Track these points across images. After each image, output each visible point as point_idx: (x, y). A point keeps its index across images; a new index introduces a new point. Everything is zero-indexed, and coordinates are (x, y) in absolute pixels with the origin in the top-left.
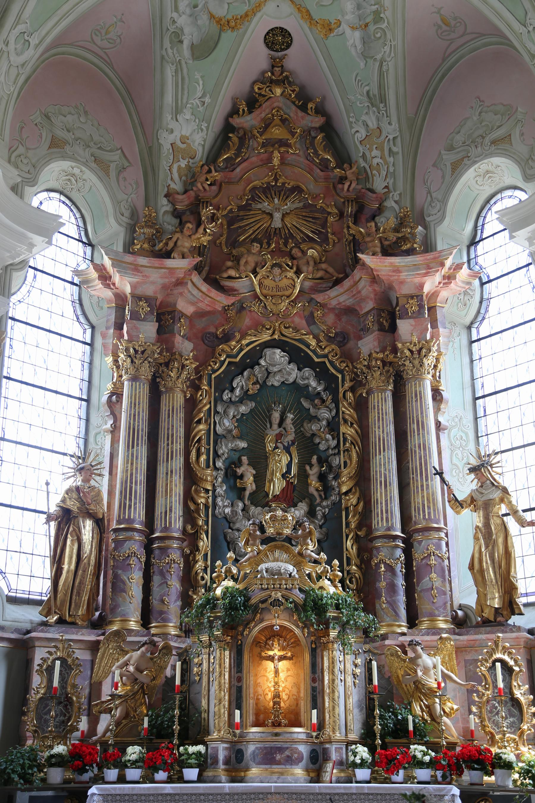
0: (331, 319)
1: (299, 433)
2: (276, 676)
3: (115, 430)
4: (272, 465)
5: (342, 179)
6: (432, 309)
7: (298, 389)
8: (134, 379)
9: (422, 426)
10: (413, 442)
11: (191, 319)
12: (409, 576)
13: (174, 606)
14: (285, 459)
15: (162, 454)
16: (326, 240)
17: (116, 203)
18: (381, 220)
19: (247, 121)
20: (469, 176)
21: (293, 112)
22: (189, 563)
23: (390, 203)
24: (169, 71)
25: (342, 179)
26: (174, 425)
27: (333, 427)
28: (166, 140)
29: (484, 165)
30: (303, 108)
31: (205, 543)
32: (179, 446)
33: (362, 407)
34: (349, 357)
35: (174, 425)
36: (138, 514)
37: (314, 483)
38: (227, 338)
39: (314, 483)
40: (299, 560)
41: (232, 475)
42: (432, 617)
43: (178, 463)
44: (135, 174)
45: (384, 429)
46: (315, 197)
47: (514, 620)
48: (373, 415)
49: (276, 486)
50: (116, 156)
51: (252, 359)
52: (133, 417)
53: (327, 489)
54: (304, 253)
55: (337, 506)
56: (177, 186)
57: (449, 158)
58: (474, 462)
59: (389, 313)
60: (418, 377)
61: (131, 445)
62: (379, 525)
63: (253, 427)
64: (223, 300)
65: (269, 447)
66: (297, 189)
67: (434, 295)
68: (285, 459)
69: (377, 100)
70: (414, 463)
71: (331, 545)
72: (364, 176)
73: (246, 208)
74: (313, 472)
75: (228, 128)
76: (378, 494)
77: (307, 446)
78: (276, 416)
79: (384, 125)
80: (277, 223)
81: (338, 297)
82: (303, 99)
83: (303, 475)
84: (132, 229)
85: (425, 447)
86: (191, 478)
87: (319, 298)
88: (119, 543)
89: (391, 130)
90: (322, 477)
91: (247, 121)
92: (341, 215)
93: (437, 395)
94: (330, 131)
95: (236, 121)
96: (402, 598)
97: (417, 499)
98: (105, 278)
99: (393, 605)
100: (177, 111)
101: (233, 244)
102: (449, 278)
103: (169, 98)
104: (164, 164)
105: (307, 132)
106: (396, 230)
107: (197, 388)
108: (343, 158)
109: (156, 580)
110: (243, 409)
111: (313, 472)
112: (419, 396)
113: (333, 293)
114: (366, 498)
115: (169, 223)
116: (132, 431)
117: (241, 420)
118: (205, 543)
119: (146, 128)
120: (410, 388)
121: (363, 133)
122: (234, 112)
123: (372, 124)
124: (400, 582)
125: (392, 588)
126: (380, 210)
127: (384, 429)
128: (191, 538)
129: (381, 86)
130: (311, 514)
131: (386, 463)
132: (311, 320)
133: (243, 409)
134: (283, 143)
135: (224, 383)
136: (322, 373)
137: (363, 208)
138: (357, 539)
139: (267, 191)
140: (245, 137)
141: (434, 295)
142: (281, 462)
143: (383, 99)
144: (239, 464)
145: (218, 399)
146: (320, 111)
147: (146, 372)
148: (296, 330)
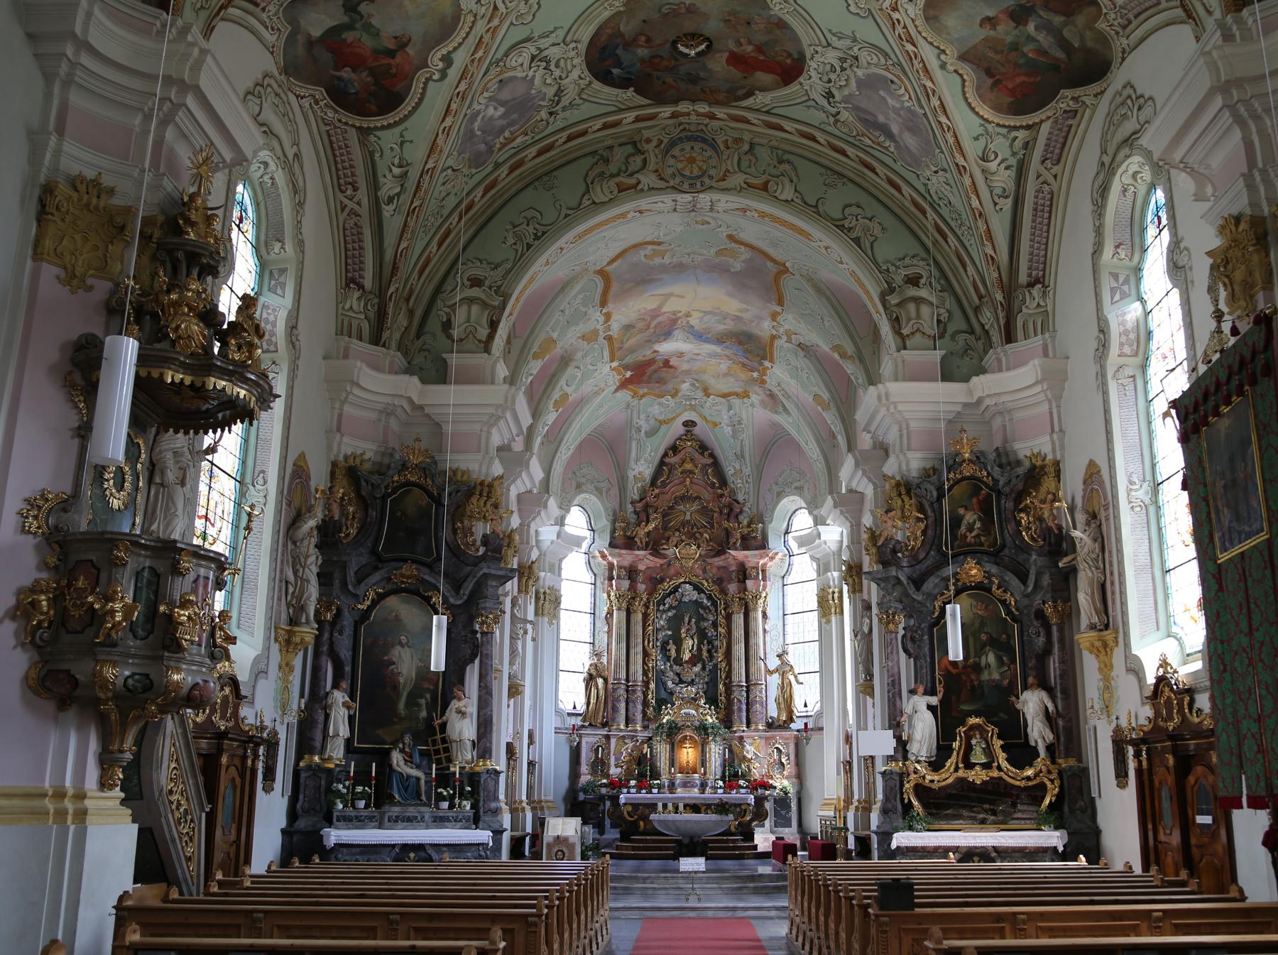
0: (714, 570)
1: (698, 627)
2: (688, 754)
3: (609, 632)
4: (685, 646)
5: (722, 496)
6: (764, 571)
7: (698, 604)
8: (619, 609)
9: (756, 634)
10: (752, 641)
11: (644, 572)
12: (748, 704)
13: (639, 717)
14: (691, 643)
15: (632, 644)
16: (712, 527)
17: (606, 509)
18: (741, 518)
19: (672, 460)
20: (785, 501)
21: (696, 455)
22: (645, 695)
23: (746, 509)
24: (634, 444)
25: (722, 496)
26: (638, 629)
27: (715, 625)
28: (631, 474)
29: (792, 498)
30: (702, 454)
31: (652, 686)
32: (640, 640)
33: (729, 618)
34: (724, 592)
35: (638, 629)
36: (623, 675)
37: (705, 654)
38: (662, 581)
39: (705, 654)
40: (697, 707)
41: (664, 648)
42: (757, 724)
43: (640, 649)
44: (615, 491)
45: (738, 632)
46: (708, 502)
47: (792, 725)
48: (734, 626)
49: (687, 656)
50: (605, 484)
51: (676, 589)
52: (619, 628)
53: (711, 657)
54: (701, 534)
55: (715, 666)
56: (636, 497)
57: (776, 489)
58: (780, 651)
59: (743, 573)
60: (755, 609)
61: (618, 642)
62: (735, 679)
63: (675, 623)
64: (661, 561)
65: (683, 635)
66: (698, 498)
67: (765, 564)
68: (691, 643)
69: (740, 457)
70: (752, 652)
71: (712, 700)
72: (733, 492)
73: (671, 508)
74: (705, 648)
75: (662, 463)
76: (735, 664)
77: (702, 635)
78: (687, 619)
79: (744, 470)
80: (688, 517)
81: (718, 561)
82: (703, 448)
83: (699, 649)
84: (614, 522)
85: (757, 644)
86: (646, 654)
87: (709, 561)
88: (614, 690)
89: (747, 471)
90: (709, 651)
91: (672, 460)
92: (721, 513)
93: (765, 615)
94: (716, 464)
95: (667, 460)
96: (744, 714)
97: (752, 670)
98: (604, 557)
99: (740, 718)
100: (637, 460)
101: (665, 528)
102: (772, 558)
103: (633, 455)
104: (630, 486)
105: (705, 466)
106: (749, 526)
107: (648, 607)
108: (724, 482)
109: (631, 705)
110: (670, 614)
111: (705, 648)
112: (756, 619)
113: (716, 559)
114: (729, 664)
115: (632, 518)
116: (619, 635)
117: (669, 620)
118: (652, 686)
119: (621, 467)
120: (752, 614)
121: (732, 471)
122: (665, 455)
123: (738, 467)
124: (744, 707)
125: (740, 710)
126: (741, 512)
127: (738, 632)
128: (646, 684)
129: (742, 451)
130: (704, 668)
131: (739, 650)
132: (704, 571)
133: (670, 614)
134: (691, 472)
135: (661, 602)
136: (710, 598)
137: (732, 510)
138: (725, 684)
139: (684, 498)
140: (672, 468)
141: (765, 564)
142: (689, 644)
143: (743, 457)
144: (668, 643)
145: (658, 610)
146: (712, 455)
147: (624, 605)
148: (697, 576)
